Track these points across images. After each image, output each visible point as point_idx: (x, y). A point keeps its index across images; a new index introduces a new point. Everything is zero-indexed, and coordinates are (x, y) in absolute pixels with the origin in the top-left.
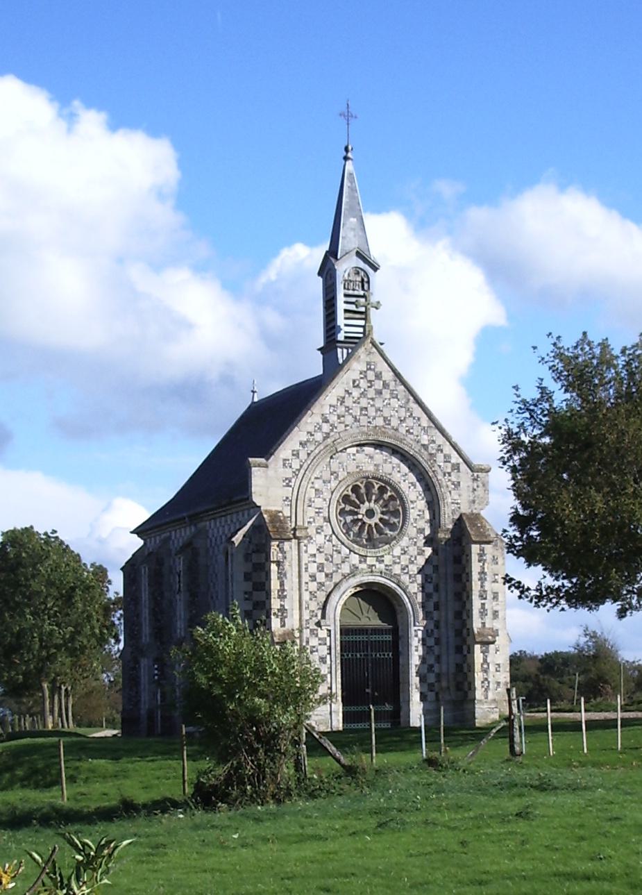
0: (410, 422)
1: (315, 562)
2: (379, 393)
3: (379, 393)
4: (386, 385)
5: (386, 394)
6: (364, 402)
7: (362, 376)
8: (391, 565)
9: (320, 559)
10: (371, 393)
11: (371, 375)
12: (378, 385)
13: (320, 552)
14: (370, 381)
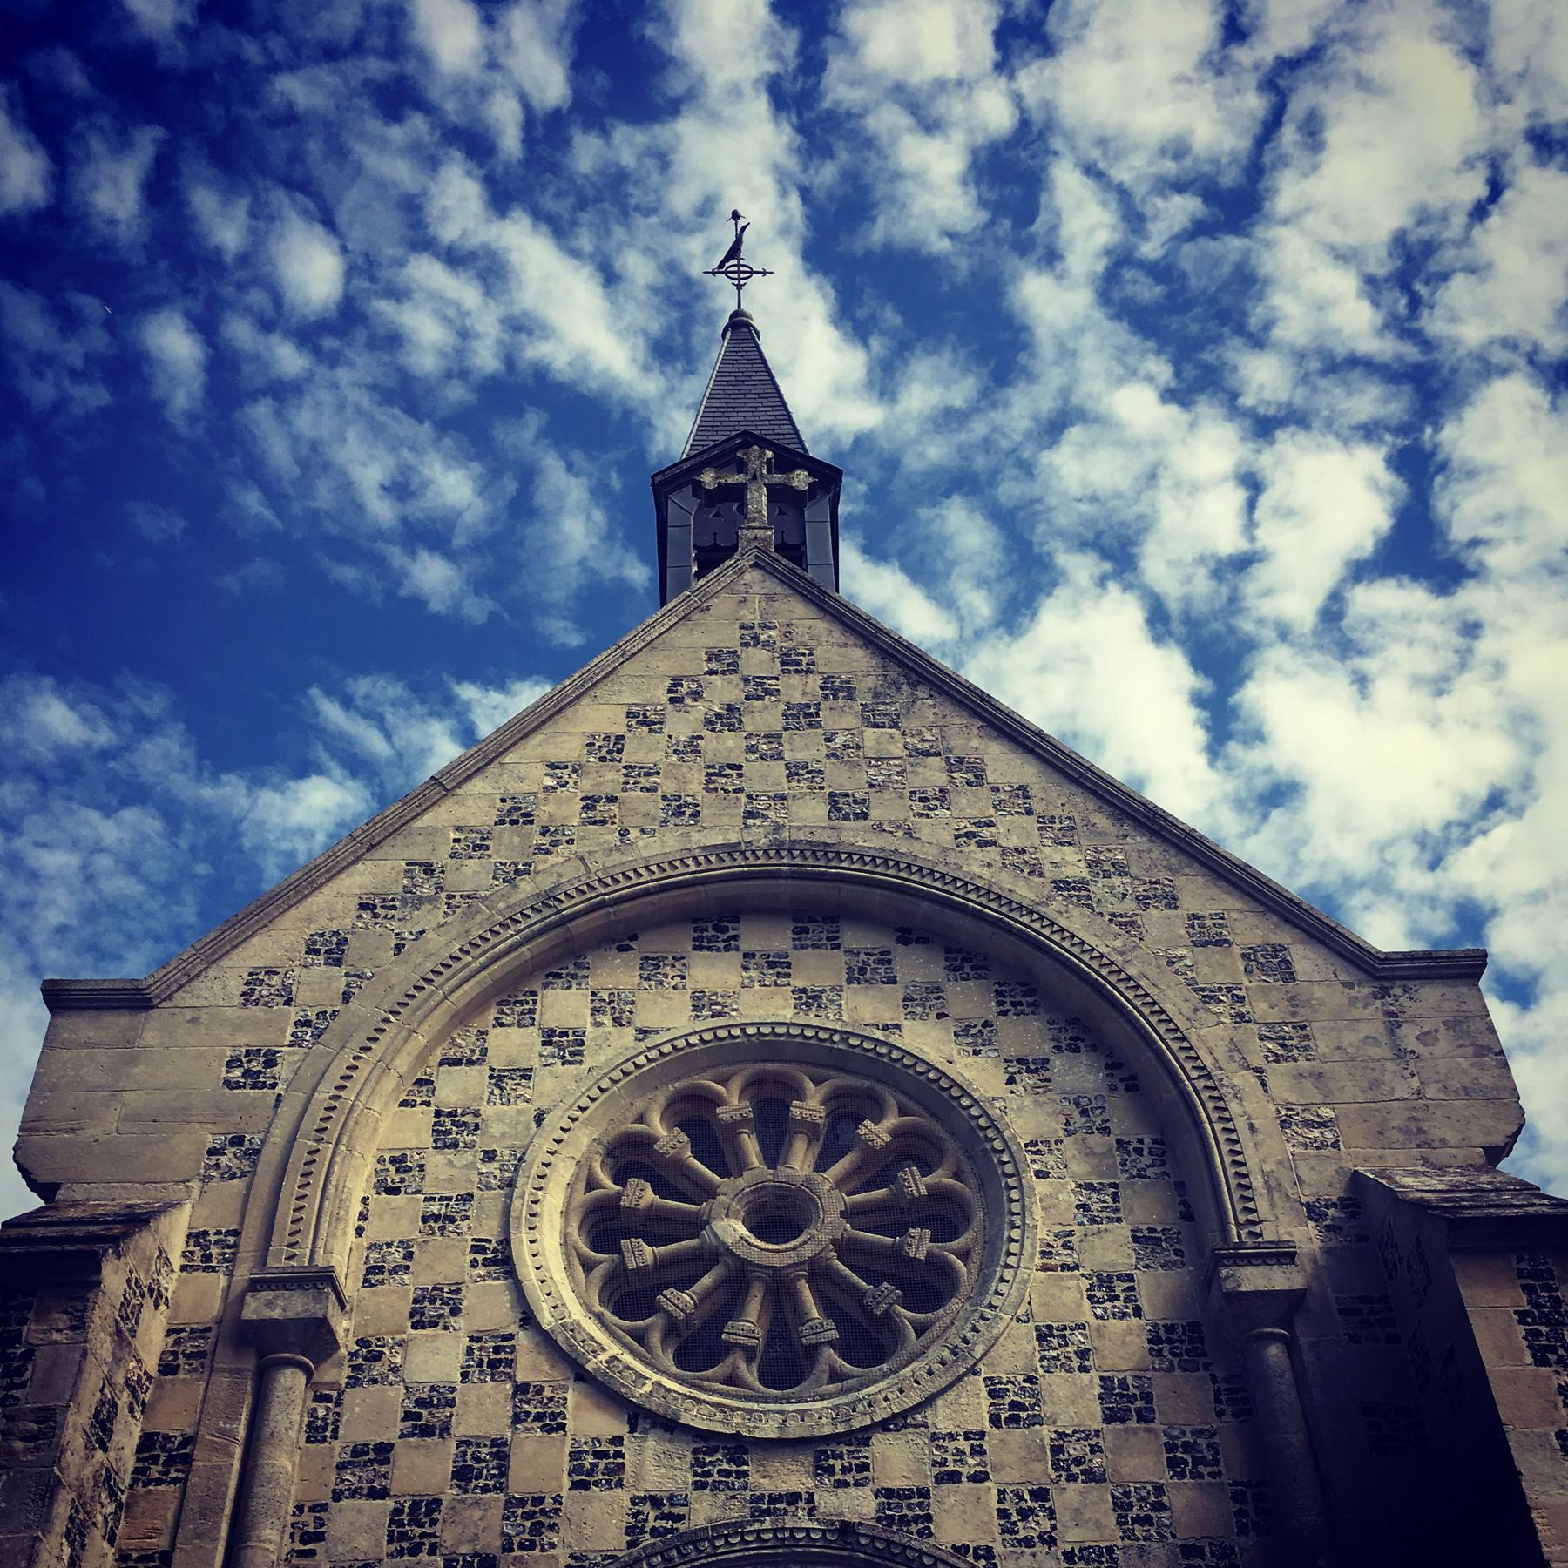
8: (924, 1493)
13: (427, 1431)
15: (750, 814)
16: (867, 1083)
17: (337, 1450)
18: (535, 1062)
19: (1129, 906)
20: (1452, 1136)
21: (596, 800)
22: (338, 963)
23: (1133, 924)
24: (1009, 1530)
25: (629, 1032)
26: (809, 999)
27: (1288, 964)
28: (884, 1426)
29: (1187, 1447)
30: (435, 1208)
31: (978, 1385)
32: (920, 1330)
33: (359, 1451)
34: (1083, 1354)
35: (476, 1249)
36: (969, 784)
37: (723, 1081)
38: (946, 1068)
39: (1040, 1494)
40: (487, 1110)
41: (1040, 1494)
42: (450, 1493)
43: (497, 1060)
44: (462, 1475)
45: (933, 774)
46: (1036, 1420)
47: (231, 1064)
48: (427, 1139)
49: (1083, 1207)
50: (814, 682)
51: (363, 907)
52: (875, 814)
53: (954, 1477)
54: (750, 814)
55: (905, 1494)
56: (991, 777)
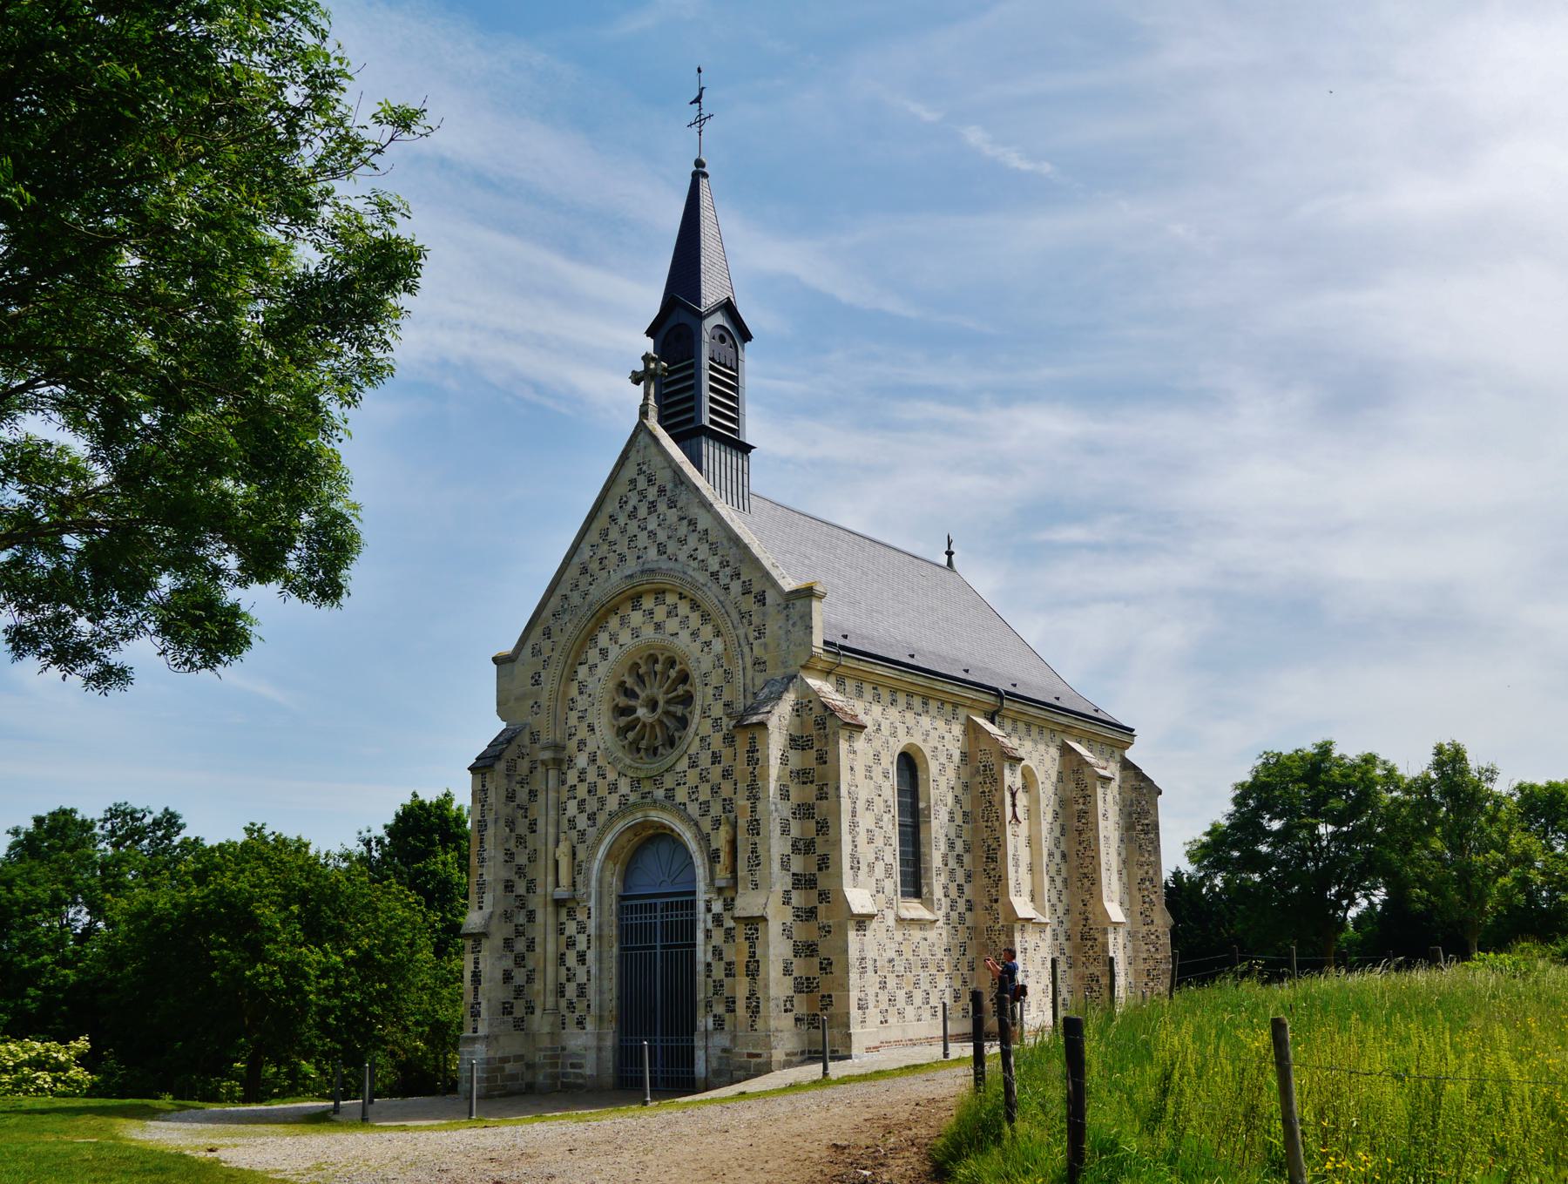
0: (693, 541)
1: (575, 798)
2: (652, 506)
3: (652, 506)
4: (662, 491)
5: (662, 507)
6: (633, 527)
7: (631, 487)
9: (582, 791)
10: (643, 511)
11: (642, 483)
12: (652, 493)
13: (581, 781)
14: (640, 493)
15: (638, 558)
16: (672, 654)
17: (566, 788)
18: (598, 661)
19: (728, 580)
20: (791, 662)
21: (601, 559)
22: (549, 638)
23: (728, 588)
24: (690, 797)
25: (618, 646)
26: (658, 626)
27: (764, 598)
28: (667, 771)
29: (727, 771)
30: (580, 714)
31: (686, 758)
32: (680, 738)
33: (571, 787)
34: (709, 744)
35: (589, 726)
36: (693, 531)
37: (641, 658)
38: (686, 649)
39: (697, 787)
40: (589, 680)
41: (697, 787)
42: (587, 797)
43: (590, 662)
44: (589, 791)
45: (683, 529)
46: (697, 766)
47: (532, 678)
48: (577, 692)
49: (714, 695)
50: (656, 488)
51: (554, 615)
52: (669, 551)
53: (679, 784)
54: (638, 558)
55: (670, 790)
56: (700, 527)
